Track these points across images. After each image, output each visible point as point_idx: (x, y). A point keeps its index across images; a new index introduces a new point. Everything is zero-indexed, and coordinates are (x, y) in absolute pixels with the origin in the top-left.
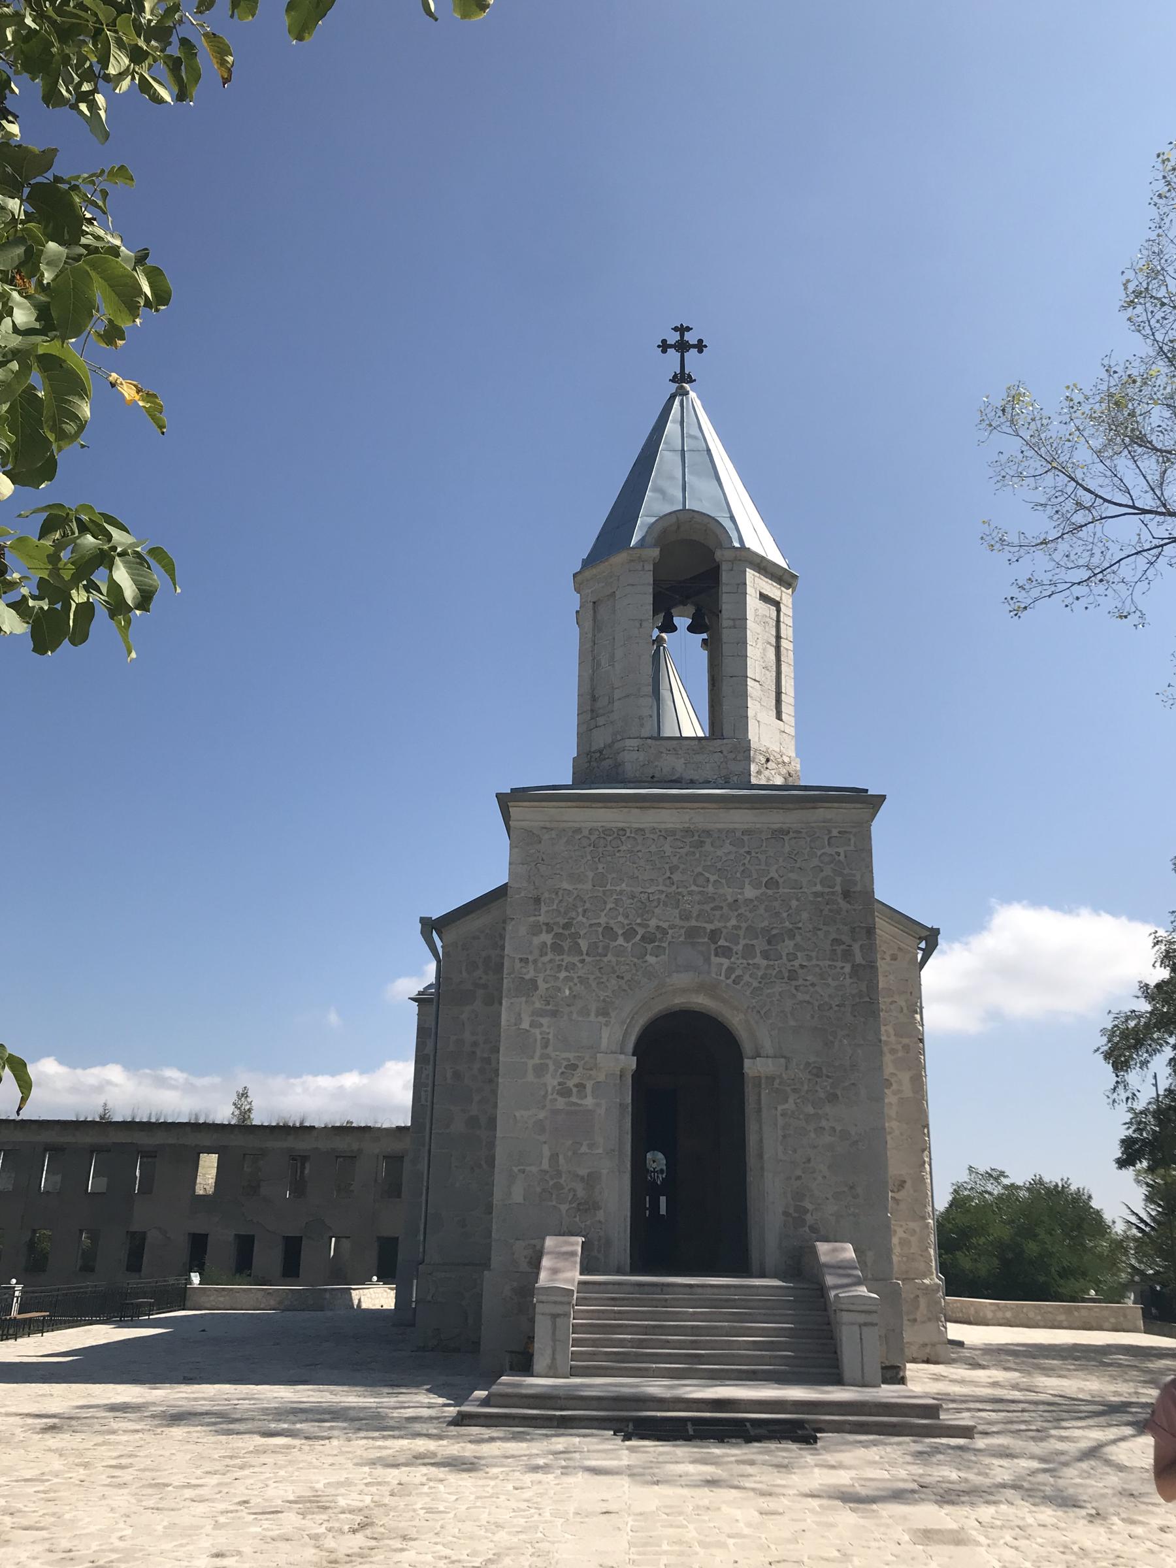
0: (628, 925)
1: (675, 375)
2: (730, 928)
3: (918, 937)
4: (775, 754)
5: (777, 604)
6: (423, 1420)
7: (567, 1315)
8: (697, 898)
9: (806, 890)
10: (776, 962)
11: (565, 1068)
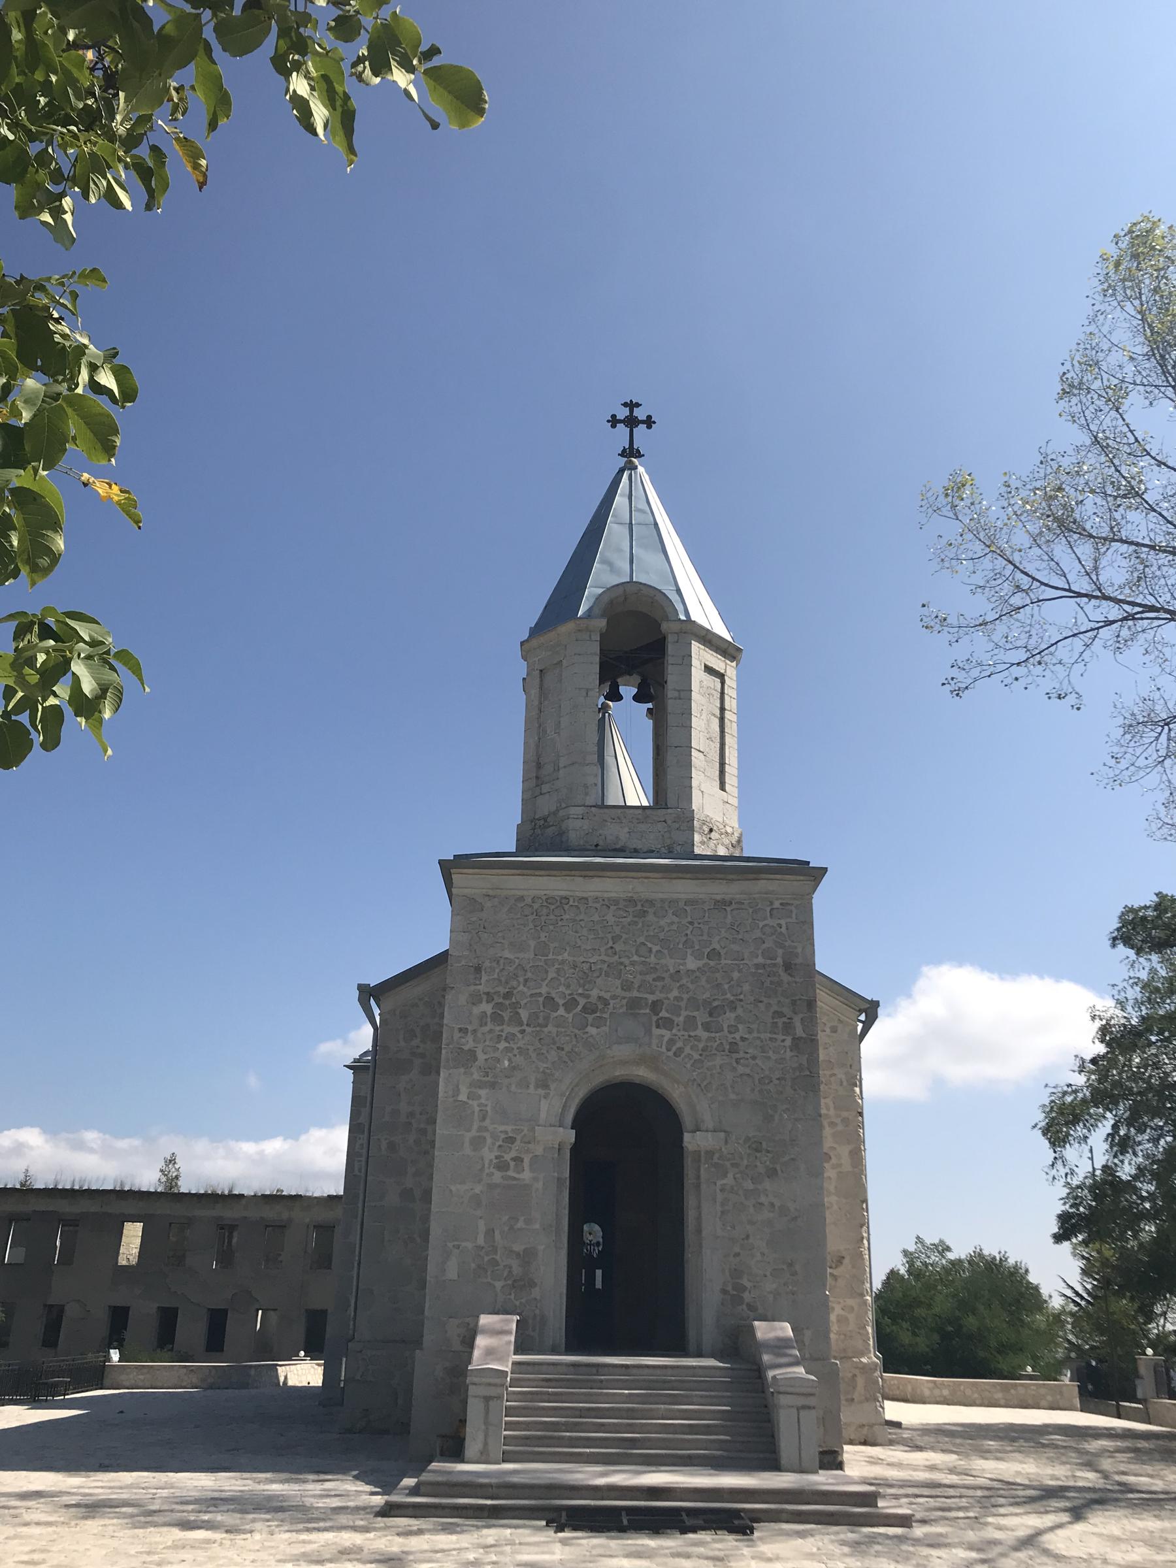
0: (570, 995)
1: (624, 450)
2: (672, 999)
3: (858, 1009)
4: (718, 824)
5: (721, 676)
6: (349, 1510)
7: (500, 1397)
10: (717, 1035)
11: (503, 1141)
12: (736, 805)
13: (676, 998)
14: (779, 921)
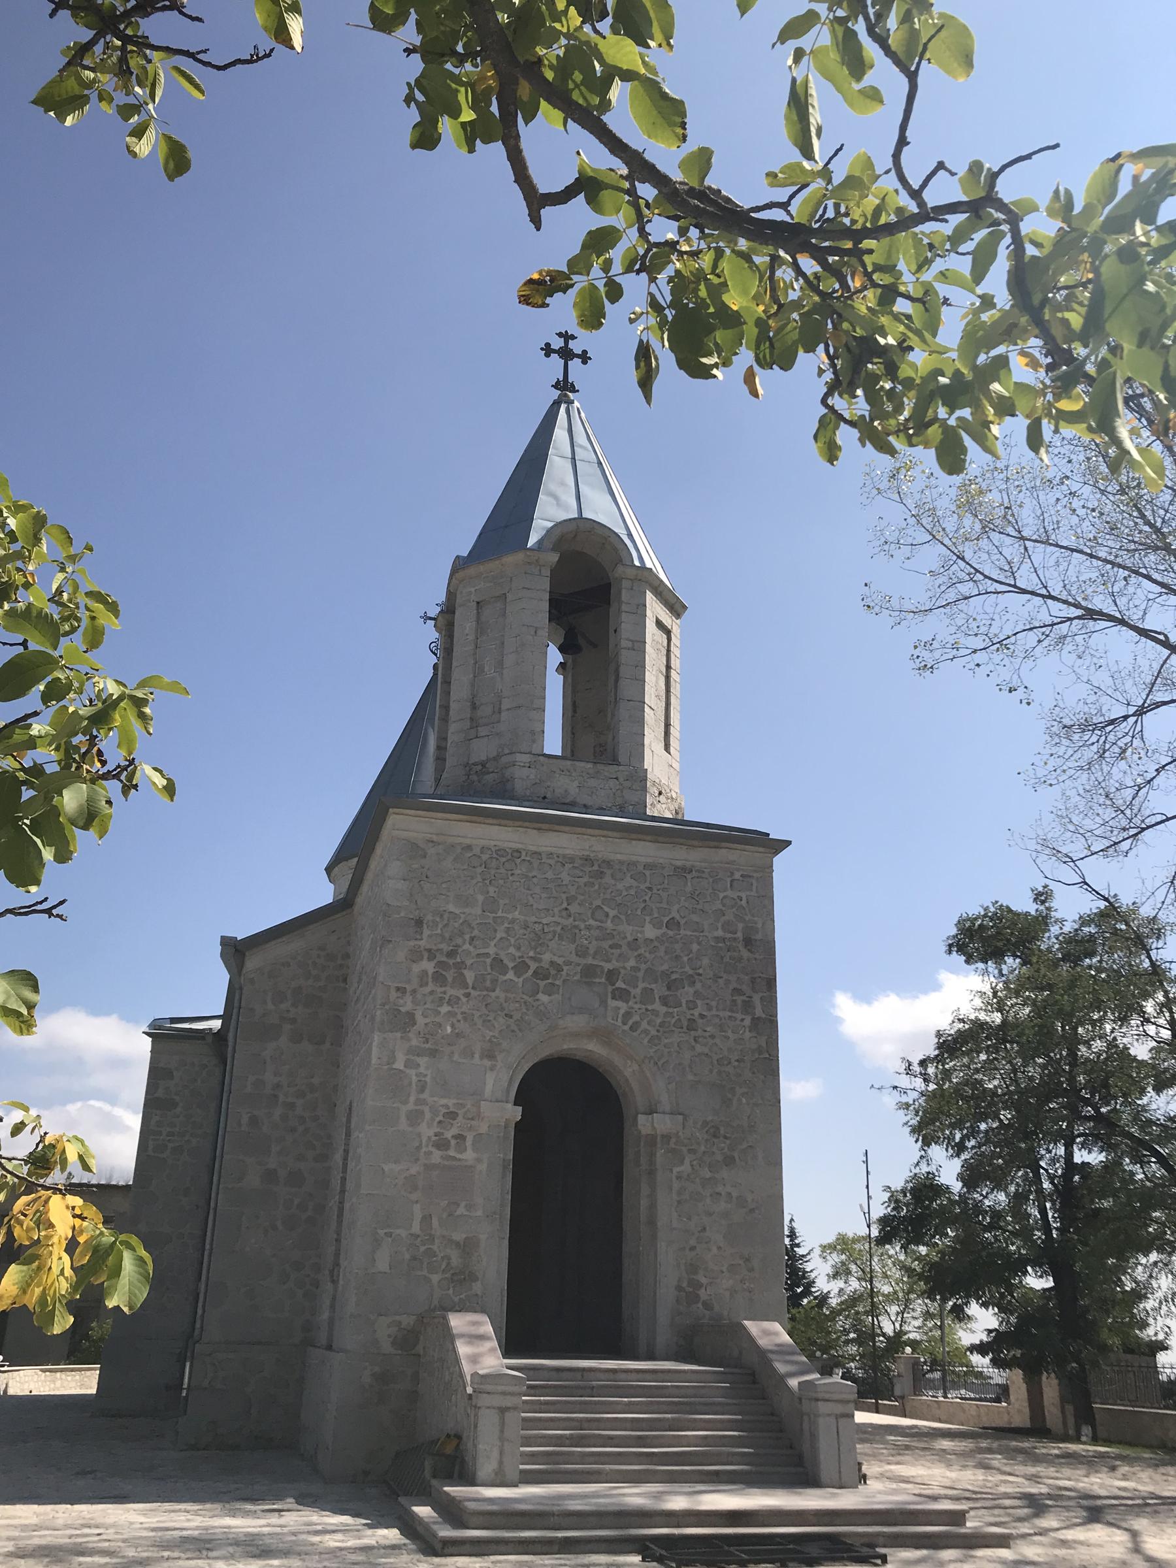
0: (519, 957)
1: (558, 382)
5: (668, 632)
8: (596, 933)
9: (707, 934)
13: (635, 969)
14: (740, 894)
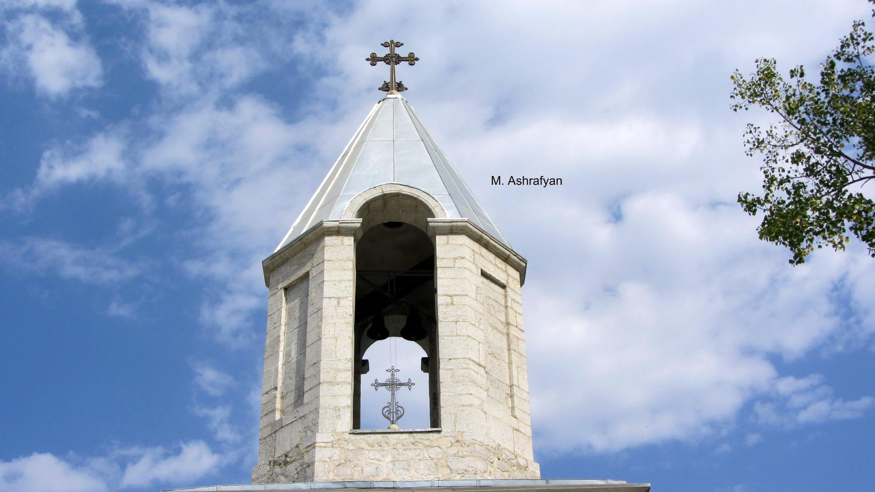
4: (508, 453)
12: (530, 435)
